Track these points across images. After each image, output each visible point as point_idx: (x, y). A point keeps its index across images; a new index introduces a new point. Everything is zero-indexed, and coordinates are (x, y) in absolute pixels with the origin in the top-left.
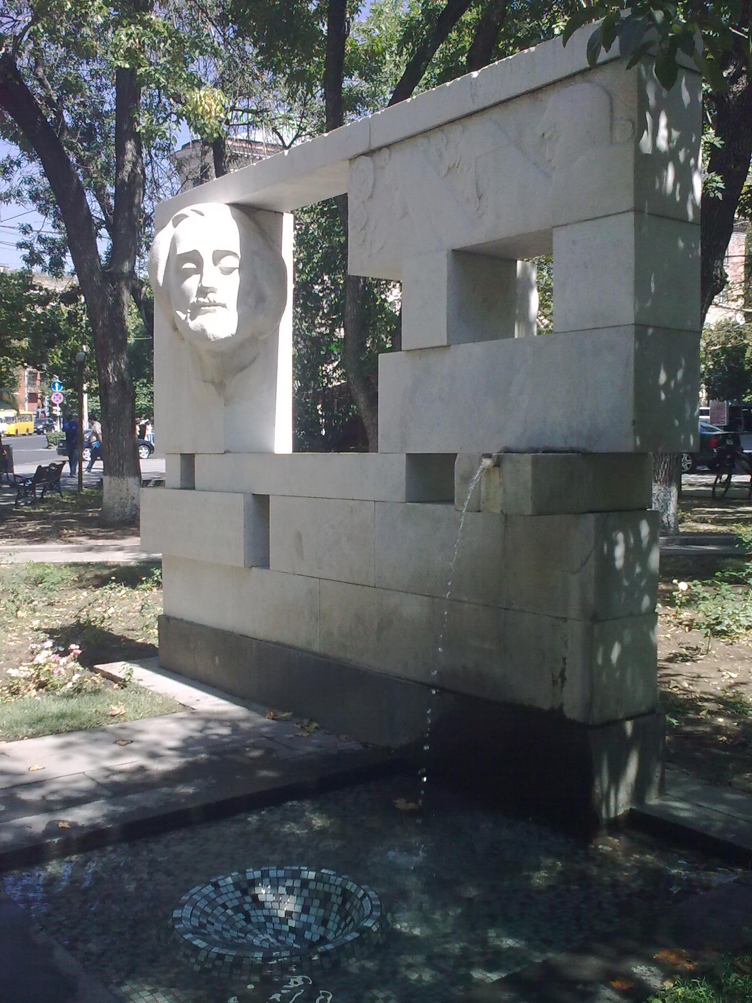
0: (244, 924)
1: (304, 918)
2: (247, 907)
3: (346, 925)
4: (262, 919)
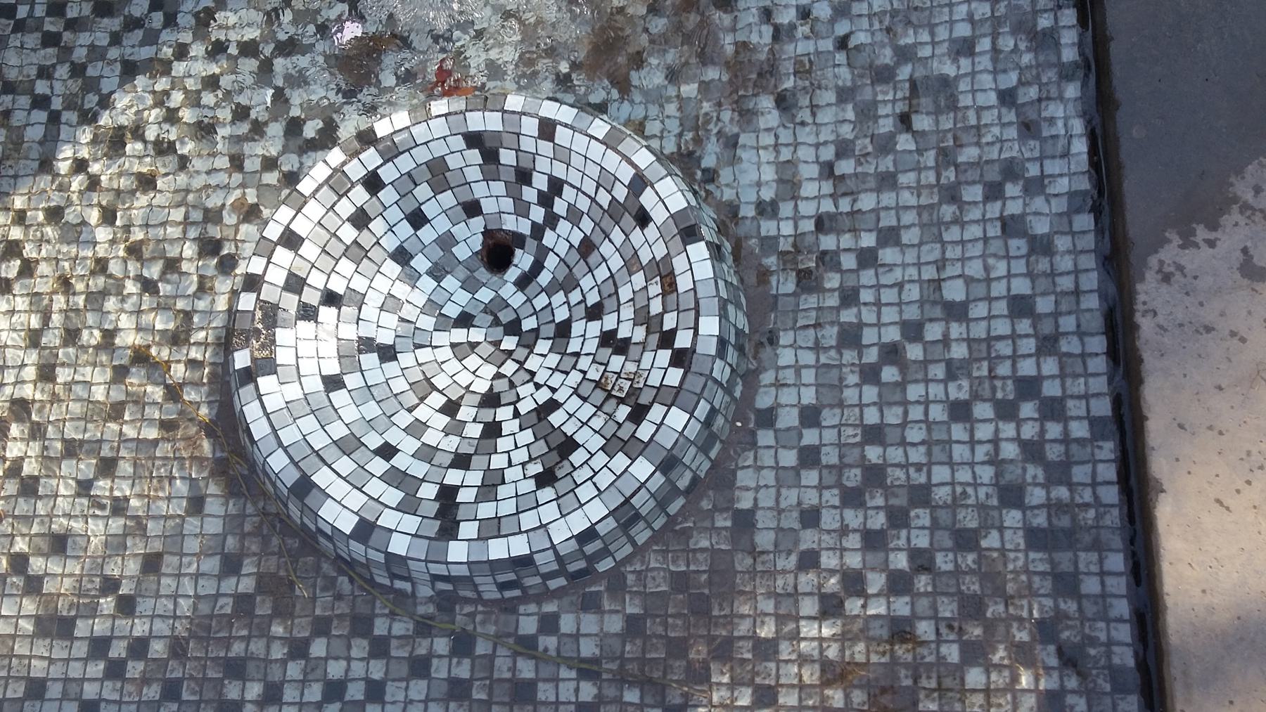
0: (391, 368)
1: (427, 234)
2: (349, 332)
4: (390, 320)
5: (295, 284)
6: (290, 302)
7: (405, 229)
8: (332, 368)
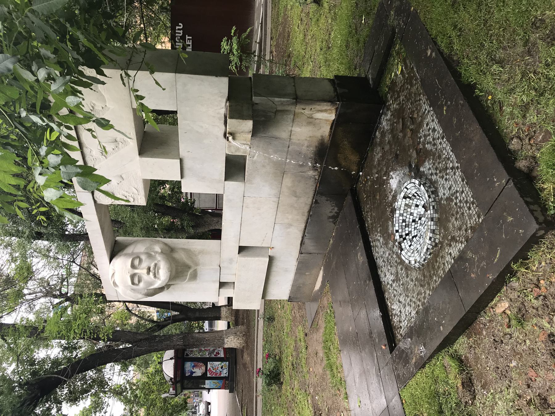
2: (411, 237)
3: (418, 195)
5: (401, 236)
6: (402, 239)
7: (411, 217)
8: (410, 244)
